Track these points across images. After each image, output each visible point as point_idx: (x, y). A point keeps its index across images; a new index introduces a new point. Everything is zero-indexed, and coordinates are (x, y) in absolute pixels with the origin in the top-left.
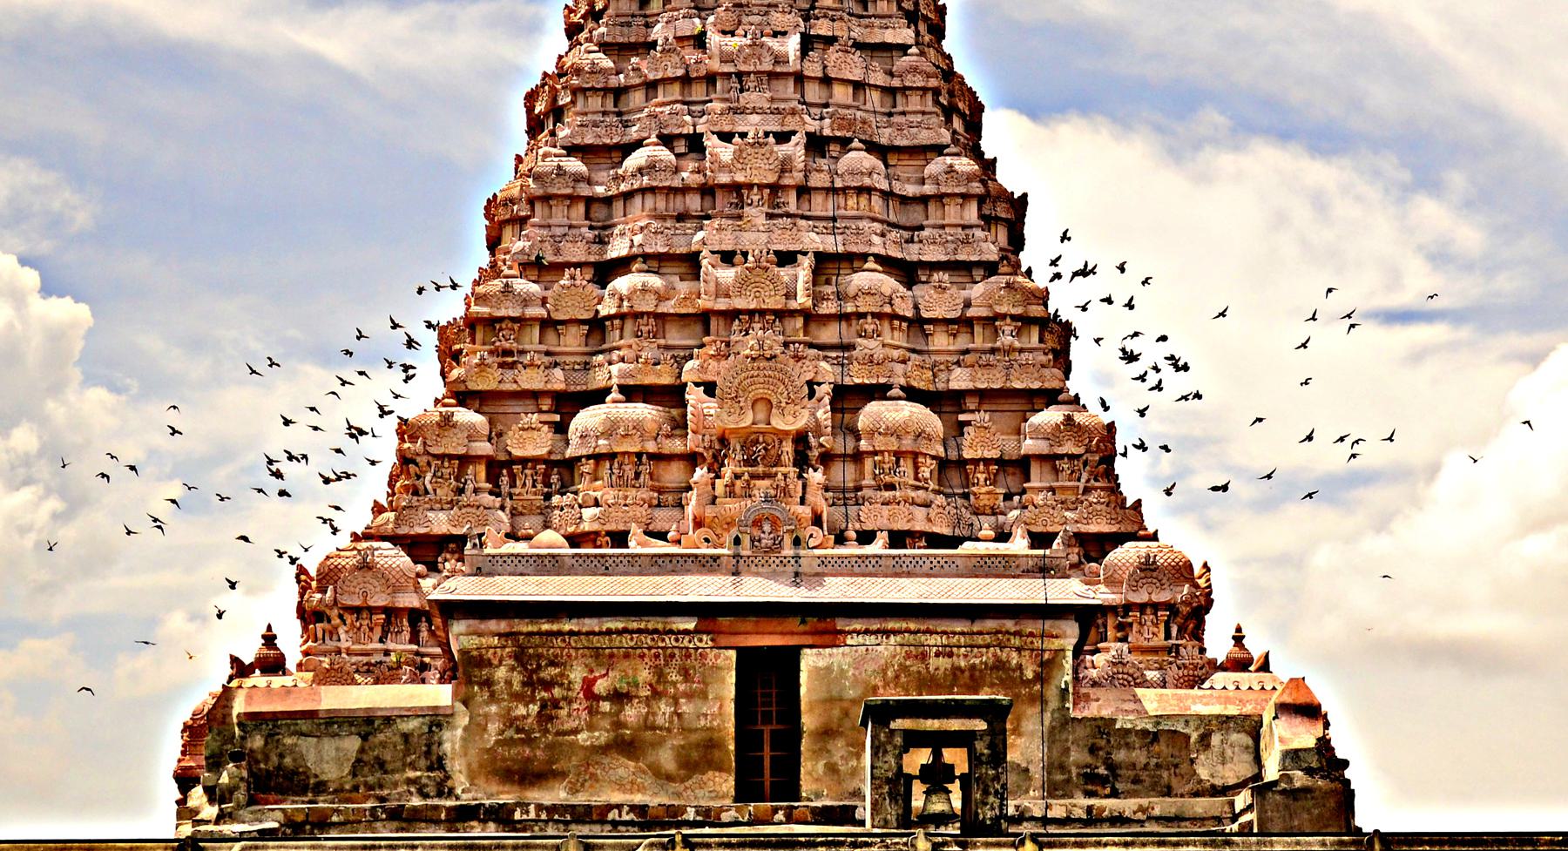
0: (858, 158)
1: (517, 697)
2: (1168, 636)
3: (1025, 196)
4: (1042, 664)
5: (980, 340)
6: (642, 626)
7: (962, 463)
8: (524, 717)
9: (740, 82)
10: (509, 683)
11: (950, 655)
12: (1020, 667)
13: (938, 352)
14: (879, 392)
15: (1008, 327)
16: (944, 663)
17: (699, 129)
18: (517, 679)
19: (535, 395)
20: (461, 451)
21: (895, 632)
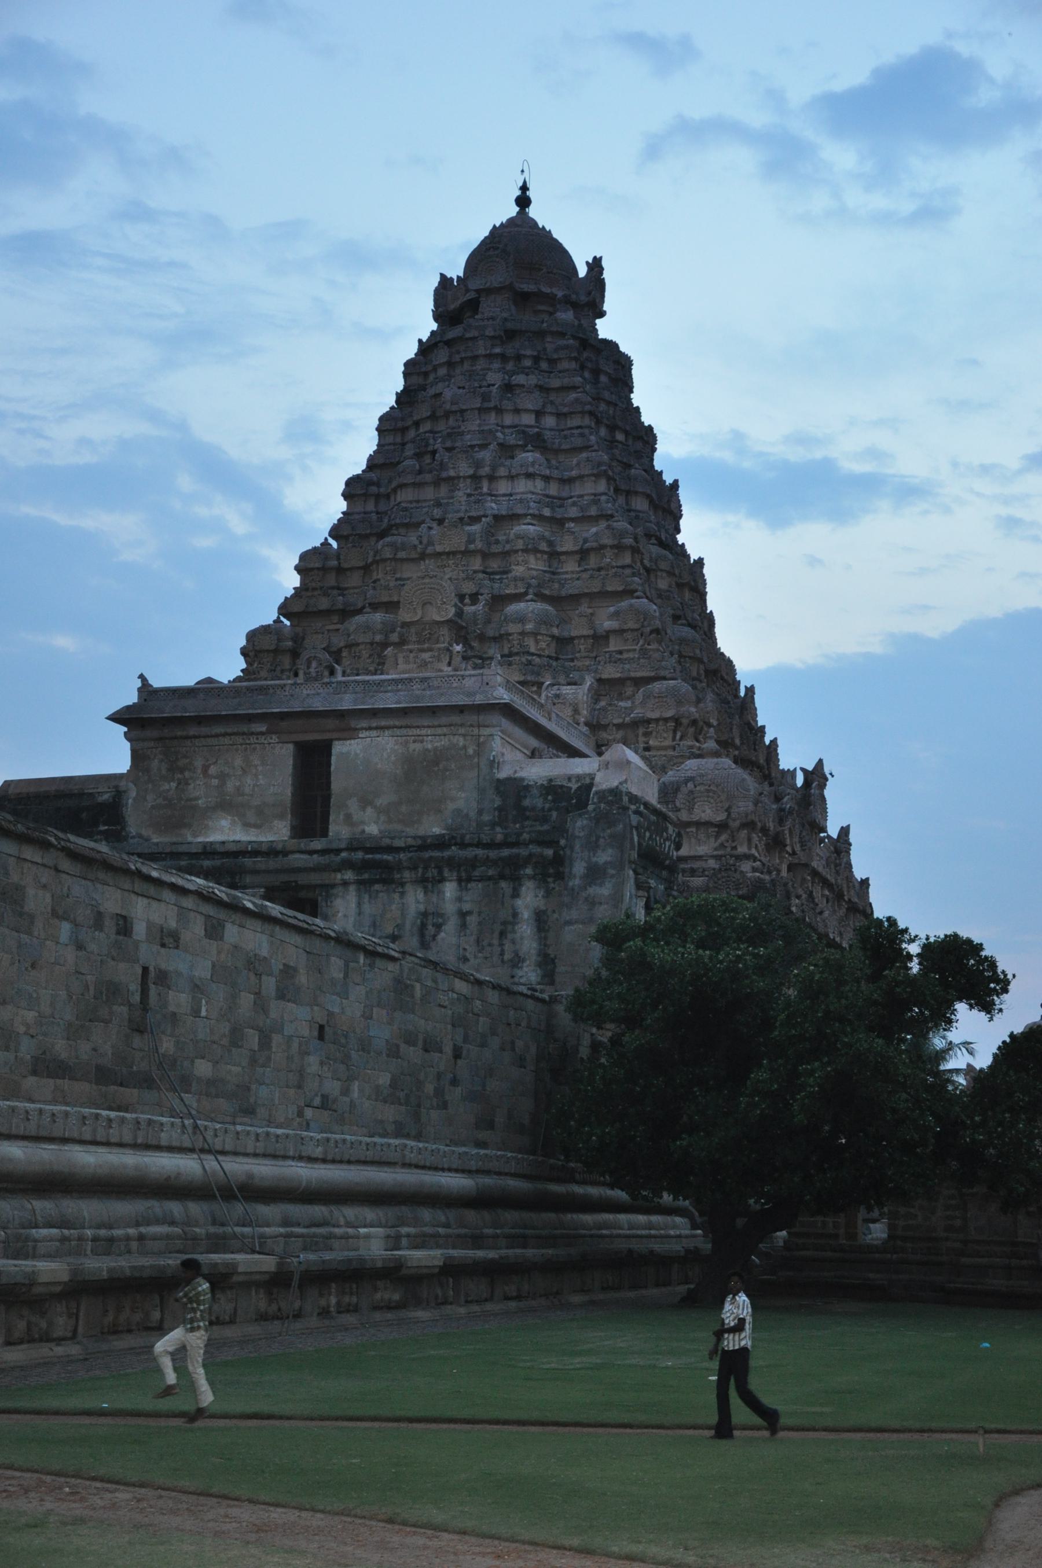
0: (530, 456)
2: (674, 739)
3: (676, 482)
4: (479, 745)
5: (593, 561)
6: (235, 730)
7: (572, 639)
8: (168, 790)
9: (462, 416)
11: (422, 742)
12: (465, 747)
13: (567, 573)
14: (517, 598)
15: (609, 553)
16: (418, 746)
21: (388, 728)
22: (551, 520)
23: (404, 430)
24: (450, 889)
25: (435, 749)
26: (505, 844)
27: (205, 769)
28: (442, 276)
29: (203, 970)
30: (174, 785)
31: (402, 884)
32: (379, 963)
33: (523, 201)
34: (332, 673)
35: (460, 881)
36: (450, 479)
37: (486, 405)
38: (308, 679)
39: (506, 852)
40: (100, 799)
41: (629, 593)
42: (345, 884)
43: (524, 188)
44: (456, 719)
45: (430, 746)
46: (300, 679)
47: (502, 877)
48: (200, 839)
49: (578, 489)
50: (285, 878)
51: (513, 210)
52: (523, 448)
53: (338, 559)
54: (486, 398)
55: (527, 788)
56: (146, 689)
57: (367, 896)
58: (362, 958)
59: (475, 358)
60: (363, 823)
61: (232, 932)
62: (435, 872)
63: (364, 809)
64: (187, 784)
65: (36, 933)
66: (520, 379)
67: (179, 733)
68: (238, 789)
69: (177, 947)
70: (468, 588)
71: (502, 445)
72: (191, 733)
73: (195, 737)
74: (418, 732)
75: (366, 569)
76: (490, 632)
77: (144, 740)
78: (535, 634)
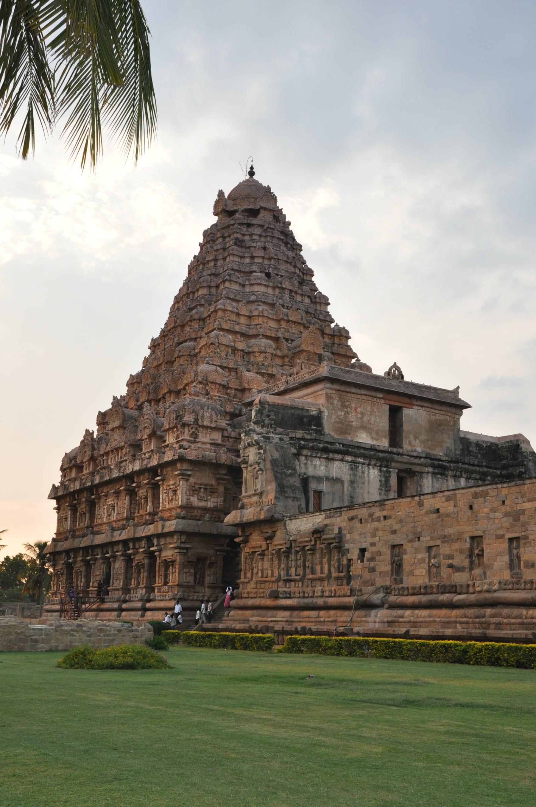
1: (339, 409)
4: (454, 421)
5: (336, 340)
8: (341, 415)
11: (435, 416)
12: (450, 422)
16: (432, 417)
17: (270, 271)
18: (339, 404)
19: (236, 333)
20: (227, 344)
25: (440, 420)
26: (478, 466)
27: (356, 409)
31: (447, 476)
33: (252, 173)
35: (466, 478)
42: (428, 473)
43: (252, 168)
45: (438, 418)
47: (481, 479)
50: (407, 466)
57: (435, 479)
59: (273, 237)
60: (415, 446)
63: (415, 439)
64: (348, 414)
67: (348, 390)
68: (369, 421)
73: (353, 393)
77: (331, 389)
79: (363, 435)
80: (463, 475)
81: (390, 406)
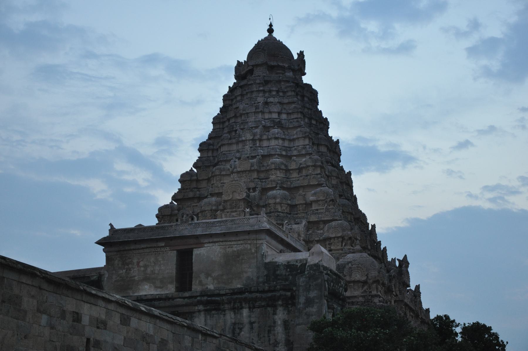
2: (342, 246)
3: (338, 140)
4: (256, 248)
5: (304, 172)
6: (151, 246)
7: (296, 205)
10: (118, 264)
12: (251, 249)
13: (293, 178)
15: (311, 169)
21: (217, 242)
22: (286, 156)
23: (224, 123)
24: (245, 312)
25: (238, 250)
27: (138, 263)
28: (238, 61)
29: (119, 341)
30: (124, 271)
31: (224, 311)
32: (209, 339)
33: (270, 30)
34: (193, 219)
35: (250, 308)
36: (243, 141)
37: (257, 110)
38: (182, 222)
39: (270, 295)
40: (92, 279)
41: (320, 185)
42: (199, 311)
43: (271, 25)
44: (247, 237)
45: (235, 249)
46: (179, 223)
47: (268, 306)
48: (135, 294)
49: (297, 143)
51: (267, 34)
52: (273, 127)
53: (197, 176)
54: (257, 108)
55: (278, 266)
56: (112, 230)
57: (208, 317)
58: (200, 336)
60: (207, 284)
61: (134, 322)
62: (239, 305)
63: (207, 278)
64: (130, 270)
65: (28, 320)
66: (271, 100)
67: (127, 248)
69: (105, 329)
70: (252, 185)
71: (264, 126)
72: (132, 248)
73: (134, 249)
74: (230, 243)
75: (209, 180)
76: (262, 204)
77: (111, 252)
78: (280, 204)
79: (146, 287)
80: (244, 305)
81: (178, 251)
